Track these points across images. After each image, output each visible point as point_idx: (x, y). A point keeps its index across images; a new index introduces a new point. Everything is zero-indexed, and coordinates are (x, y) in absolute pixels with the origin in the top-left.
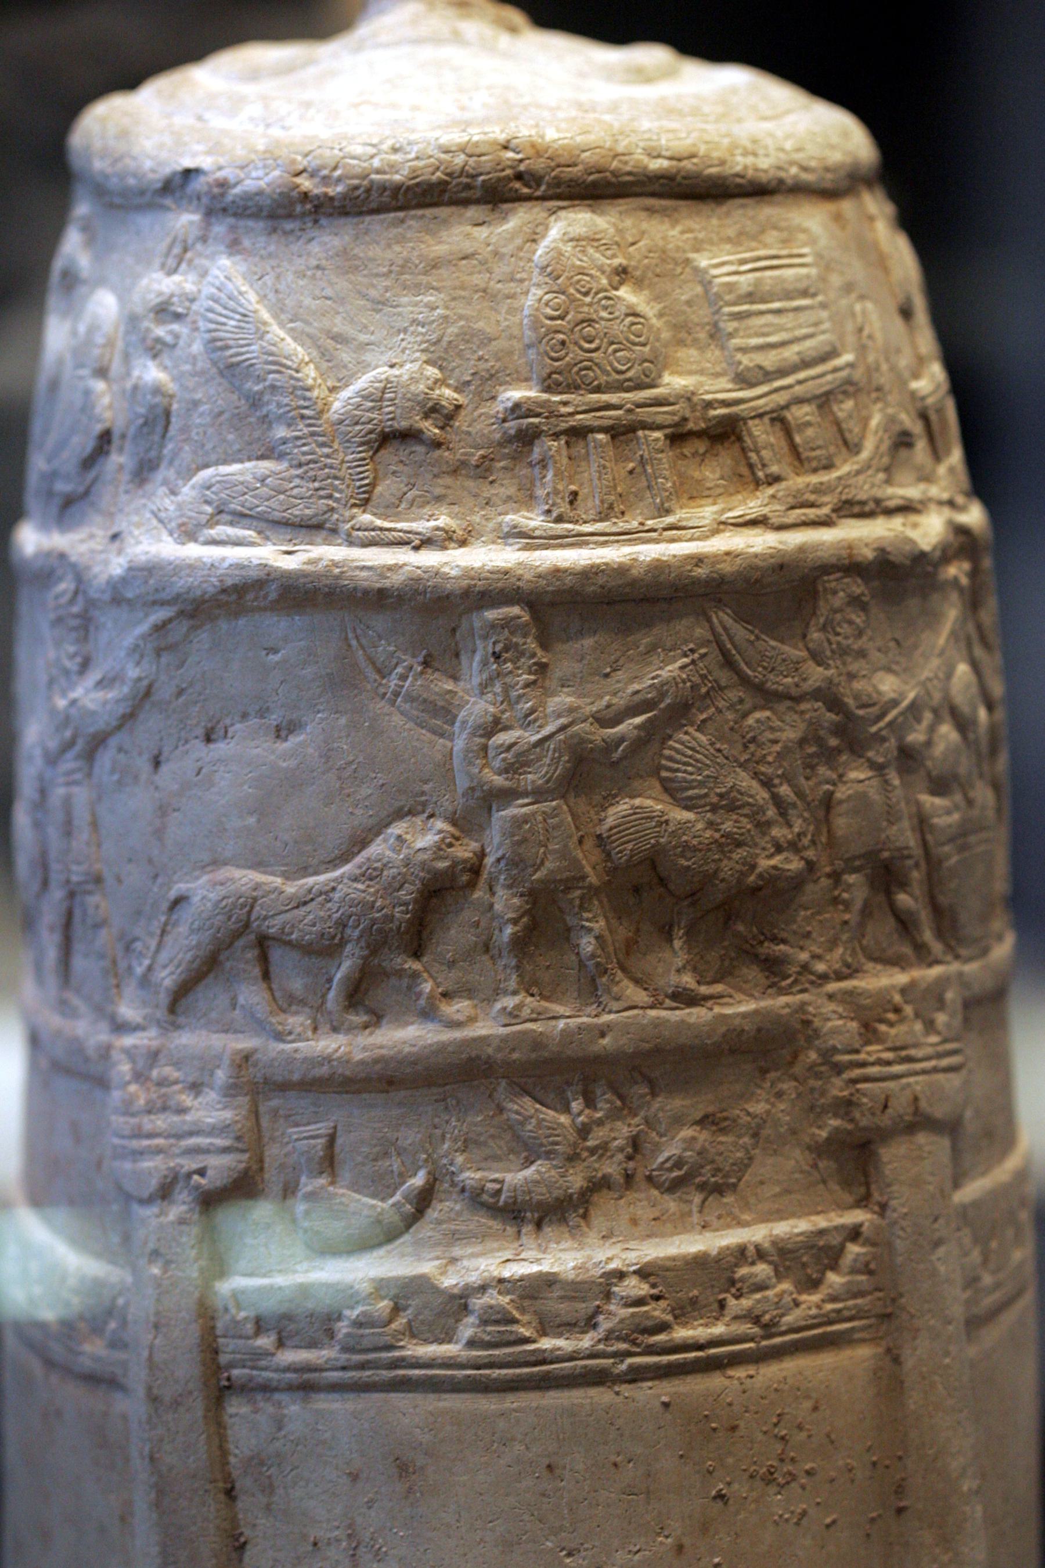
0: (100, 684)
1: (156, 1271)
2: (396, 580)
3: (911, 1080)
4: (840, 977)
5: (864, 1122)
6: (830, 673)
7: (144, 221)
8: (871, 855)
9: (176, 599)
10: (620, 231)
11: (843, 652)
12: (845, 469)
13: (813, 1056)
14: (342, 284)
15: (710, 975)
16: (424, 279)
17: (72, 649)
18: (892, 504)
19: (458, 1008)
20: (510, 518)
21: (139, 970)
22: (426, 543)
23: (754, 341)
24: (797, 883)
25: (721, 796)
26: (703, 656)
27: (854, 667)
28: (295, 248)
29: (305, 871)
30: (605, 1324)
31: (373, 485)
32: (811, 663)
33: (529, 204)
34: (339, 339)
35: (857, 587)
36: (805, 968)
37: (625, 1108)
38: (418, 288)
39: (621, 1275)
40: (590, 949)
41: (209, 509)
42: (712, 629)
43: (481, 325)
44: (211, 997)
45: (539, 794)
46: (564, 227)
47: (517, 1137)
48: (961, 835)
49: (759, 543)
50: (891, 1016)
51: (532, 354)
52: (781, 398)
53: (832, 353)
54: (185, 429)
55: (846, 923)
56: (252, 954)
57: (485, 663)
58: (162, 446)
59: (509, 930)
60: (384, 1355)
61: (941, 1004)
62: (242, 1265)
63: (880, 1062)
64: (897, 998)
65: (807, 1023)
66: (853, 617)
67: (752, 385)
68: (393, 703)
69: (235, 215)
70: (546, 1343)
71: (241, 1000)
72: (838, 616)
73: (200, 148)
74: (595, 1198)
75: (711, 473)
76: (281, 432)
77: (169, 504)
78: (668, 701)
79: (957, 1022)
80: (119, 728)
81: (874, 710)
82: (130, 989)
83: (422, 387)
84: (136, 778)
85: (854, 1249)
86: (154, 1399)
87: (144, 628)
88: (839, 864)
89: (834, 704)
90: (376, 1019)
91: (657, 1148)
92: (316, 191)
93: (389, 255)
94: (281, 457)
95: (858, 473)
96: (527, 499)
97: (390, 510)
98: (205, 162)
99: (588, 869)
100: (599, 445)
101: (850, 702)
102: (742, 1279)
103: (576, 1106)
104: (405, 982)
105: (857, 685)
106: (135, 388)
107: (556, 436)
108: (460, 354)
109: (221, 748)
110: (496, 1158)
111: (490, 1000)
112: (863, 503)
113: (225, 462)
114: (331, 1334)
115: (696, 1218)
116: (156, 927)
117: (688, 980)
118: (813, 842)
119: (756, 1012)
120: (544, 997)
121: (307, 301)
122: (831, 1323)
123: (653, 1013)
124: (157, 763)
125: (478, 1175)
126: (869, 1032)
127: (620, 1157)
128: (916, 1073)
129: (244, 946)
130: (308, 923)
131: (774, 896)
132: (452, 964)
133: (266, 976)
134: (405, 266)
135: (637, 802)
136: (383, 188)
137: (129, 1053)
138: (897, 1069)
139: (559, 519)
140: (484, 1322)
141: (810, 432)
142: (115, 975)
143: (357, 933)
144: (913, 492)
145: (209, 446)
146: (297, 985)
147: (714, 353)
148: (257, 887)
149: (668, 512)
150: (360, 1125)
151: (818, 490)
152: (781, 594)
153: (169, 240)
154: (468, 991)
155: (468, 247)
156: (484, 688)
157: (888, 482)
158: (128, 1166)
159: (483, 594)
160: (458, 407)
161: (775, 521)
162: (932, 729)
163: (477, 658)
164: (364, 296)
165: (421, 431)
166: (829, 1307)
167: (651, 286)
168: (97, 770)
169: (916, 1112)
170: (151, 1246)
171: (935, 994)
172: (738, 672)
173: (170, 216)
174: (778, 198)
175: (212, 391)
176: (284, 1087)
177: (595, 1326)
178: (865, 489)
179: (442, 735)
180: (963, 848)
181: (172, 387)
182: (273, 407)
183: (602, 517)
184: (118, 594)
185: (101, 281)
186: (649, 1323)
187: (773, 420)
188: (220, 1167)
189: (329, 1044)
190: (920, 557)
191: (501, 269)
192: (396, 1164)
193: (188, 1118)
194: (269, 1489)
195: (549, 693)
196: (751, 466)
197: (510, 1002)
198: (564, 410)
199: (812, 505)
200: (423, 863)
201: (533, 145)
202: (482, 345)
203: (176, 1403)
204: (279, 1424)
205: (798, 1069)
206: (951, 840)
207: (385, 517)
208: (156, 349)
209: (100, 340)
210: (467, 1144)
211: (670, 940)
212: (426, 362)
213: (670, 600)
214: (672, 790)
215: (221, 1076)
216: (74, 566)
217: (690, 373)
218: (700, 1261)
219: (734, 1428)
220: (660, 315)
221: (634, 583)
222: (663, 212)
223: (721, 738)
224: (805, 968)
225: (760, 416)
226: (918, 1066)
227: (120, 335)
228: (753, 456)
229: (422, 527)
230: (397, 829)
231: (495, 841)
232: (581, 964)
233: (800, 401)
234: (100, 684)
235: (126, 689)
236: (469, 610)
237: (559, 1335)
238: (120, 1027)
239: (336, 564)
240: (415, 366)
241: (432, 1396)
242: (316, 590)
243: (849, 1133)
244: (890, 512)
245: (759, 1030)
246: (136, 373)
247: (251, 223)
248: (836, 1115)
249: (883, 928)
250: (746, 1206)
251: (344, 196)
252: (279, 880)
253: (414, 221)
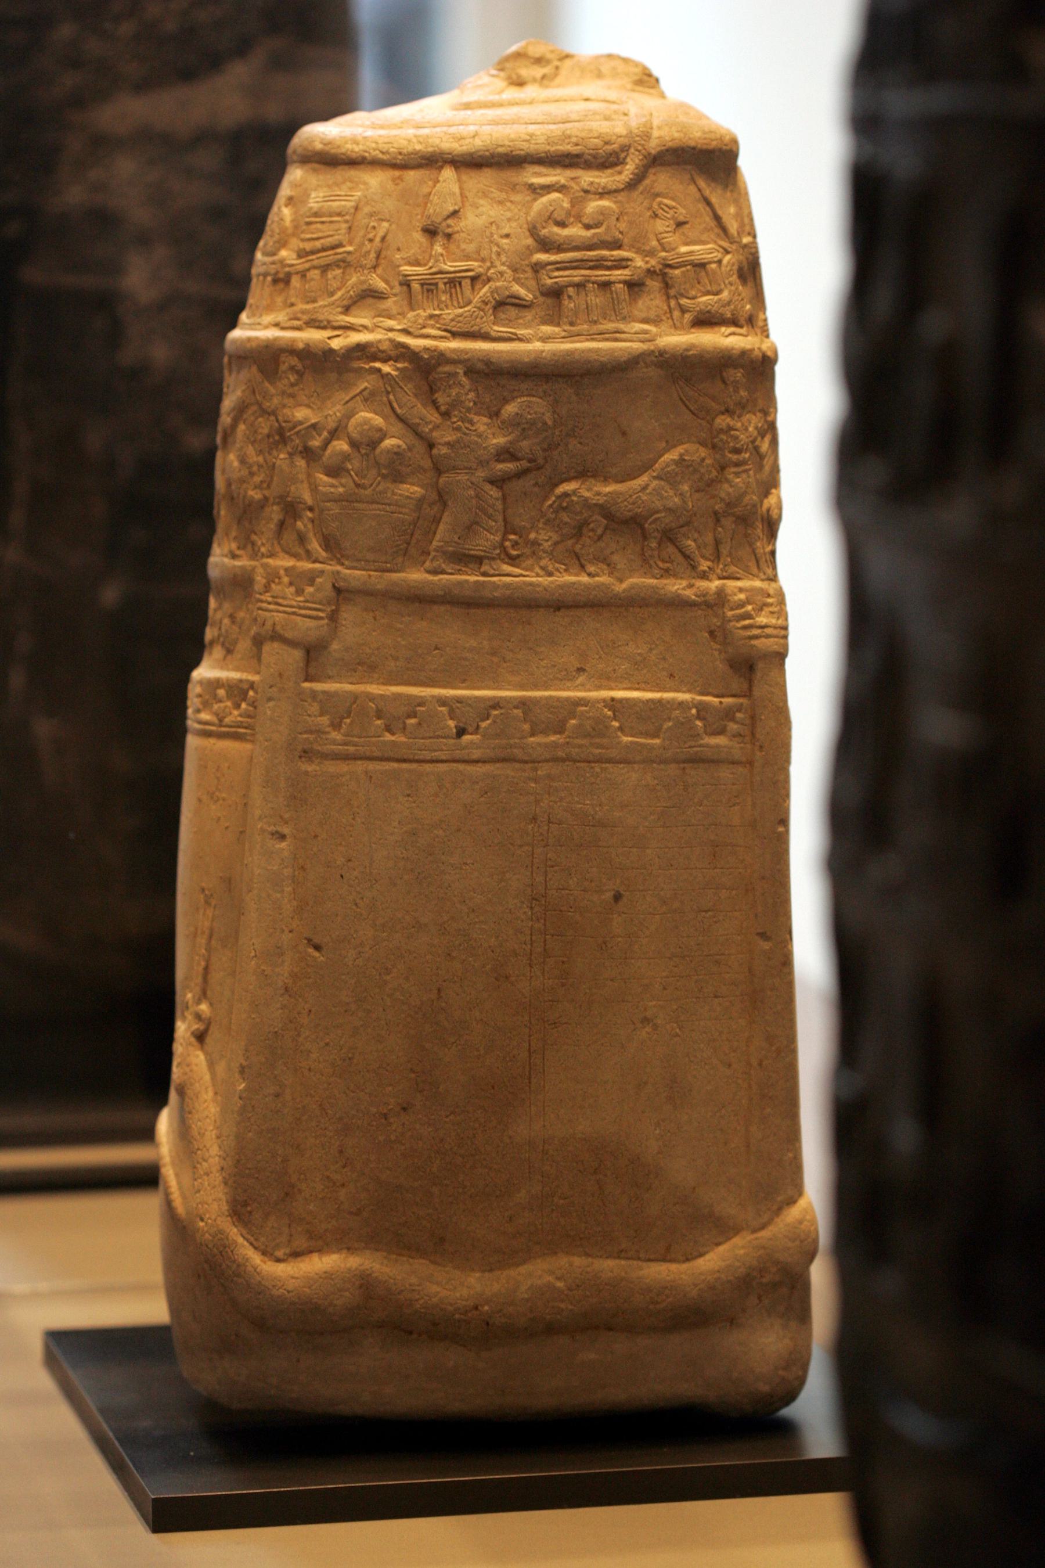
3: (275, 614)
18: (335, 324)
23: (309, 236)
27: (286, 401)
35: (294, 361)
50: (277, 580)
52: (307, 265)
53: (340, 245)
61: (311, 582)
64: (282, 572)
75: (279, 300)
81: (290, 425)
95: (325, 306)
112: (321, 321)
122: (239, 727)
128: (278, 611)
138: (272, 607)
141: (312, 283)
151: (303, 312)
162: (327, 443)
166: (239, 719)
169: (273, 630)
171: (311, 578)
174: (362, 166)
206: (335, 501)
225: (297, 273)
226: (281, 608)
233: (315, 267)
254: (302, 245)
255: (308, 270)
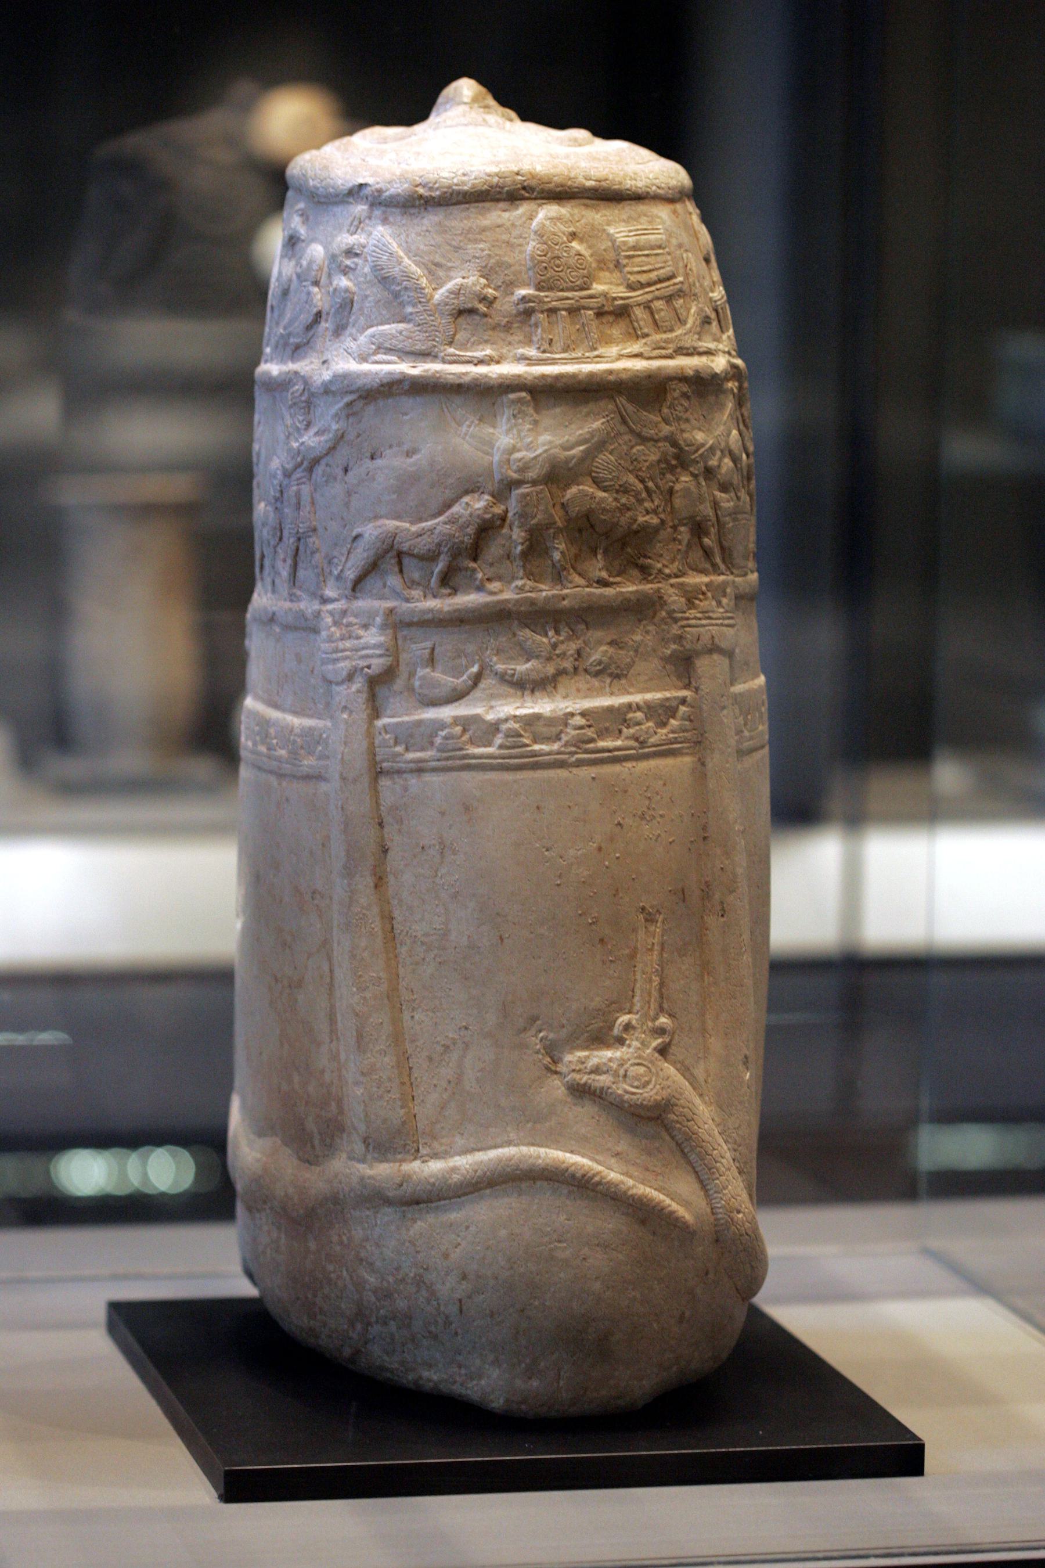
0: (317, 434)
1: (345, 716)
2: (467, 379)
4: (677, 576)
5: (688, 647)
6: (673, 429)
7: (338, 210)
8: (692, 518)
9: (357, 390)
10: (572, 215)
11: (679, 419)
12: (679, 332)
13: (664, 614)
14: (439, 239)
15: (615, 573)
16: (478, 237)
17: (301, 418)
18: (701, 350)
19: (495, 586)
20: (521, 351)
21: (336, 573)
22: (481, 362)
23: (636, 269)
24: (656, 530)
25: (620, 486)
26: (612, 419)
27: (683, 426)
28: (415, 221)
29: (421, 520)
30: (565, 738)
31: (454, 335)
32: (663, 424)
33: (528, 202)
34: (437, 265)
35: (685, 388)
36: (660, 571)
37: (574, 635)
38: (476, 241)
39: (572, 715)
40: (558, 558)
41: (374, 347)
42: (617, 406)
43: (506, 259)
44: (373, 583)
45: (534, 483)
46: (546, 213)
47: (523, 649)
48: (735, 513)
49: (639, 365)
50: (701, 597)
51: (531, 273)
52: (649, 297)
54: (361, 309)
55: (679, 550)
56: (393, 561)
57: (509, 420)
58: (349, 317)
59: (519, 548)
60: (458, 753)
62: (388, 712)
63: (695, 618)
64: (704, 588)
65: (661, 598)
66: (683, 402)
67: (634, 290)
68: (464, 439)
69: (386, 206)
70: (537, 747)
71: (389, 583)
72: (676, 402)
73: (365, 174)
74: (559, 679)
75: (616, 332)
76: (409, 309)
77: (353, 345)
78: (596, 439)
79: (732, 603)
80: (326, 454)
81: (694, 448)
82: (331, 582)
83: (478, 288)
84: (335, 479)
85: (683, 709)
86: (344, 779)
87: (341, 404)
88: (676, 522)
89: (674, 444)
90: (455, 591)
91: (589, 655)
92: (426, 194)
93: (462, 225)
94: (409, 321)
95: (685, 334)
96: (529, 342)
97: (463, 346)
98: (370, 180)
99: (557, 519)
100: (562, 316)
101: (681, 442)
102: (630, 719)
103: (551, 633)
104: (469, 573)
105: (686, 435)
106: (335, 290)
107: (542, 312)
108: (496, 273)
109: (379, 462)
110: (512, 658)
111: (510, 582)
112: (688, 349)
113: (382, 324)
114: (432, 744)
115: (607, 690)
116: (345, 551)
117: (604, 574)
118: (664, 511)
119: (637, 591)
120: (536, 581)
121: (422, 247)
122: (672, 743)
123: (588, 590)
124: (346, 470)
125: (504, 667)
126: (690, 603)
127: (571, 659)
129: (391, 557)
130: (423, 545)
131: (644, 536)
132: (492, 565)
133: (401, 571)
134: (470, 230)
135: (581, 487)
136: (459, 193)
137: (331, 613)
138: (704, 622)
139: (544, 352)
140: (507, 736)
141: (662, 314)
142: (322, 577)
143: (446, 549)
144: (712, 345)
145: (373, 317)
146: (416, 576)
147: (617, 275)
148: (397, 528)
149: (595, 349)
150: (446, 642)
152: (648, 391)
153: (351, 219)
154: (500, 578)
155: (499, 221)
156: (508, 431)
157: (699, 339)
158: (330, 667)
159: (508, 386)
160: (495, 298)
161: (646, 355)
162: (720, 460)
163: (505, 417)
164: (450, 245)
165: (477, 309)
166: (671, 735)
167: (587, 242)
168: (314, 476)
169: (713, 643)
170: (343, 704)
172: (629, 427)
173: (351, 206)
175: (375, 290)
176: (410, 625)
177: (560, 739)
178: (689, 342)
179: (488, 454)
180: (735, 520)
181: (354, 289)
182: (406, 298)
183: (564, 351)
184: (327, 390)
185: (314, 240)
186: (586, 738)
187: (645, 307)
188: (378, 664)
189: (432, 603)
190: (715, 376)
191: (516, 232)
192: (464, 661)
193: (362, 641)
194: (400, 821)
195: (539, 434)
196: (634, 329)
197: (520, 583)
198: (546, 300)
199: (664, 348)
200: (479, 516)
201: (531, 173)
202: (507, 268)
203: (355, 781)
204: (406, 789)
205: (656, 620)
206: (730, 515)
207: (460, 350)
208: (345, 271)
209: (315, 267)
210: (498, 652)
211: (596, 555)
212: (481, 276)
213: (596, 391)
214: (597, 482)
215: (378, 620)
216: (303, 377)
217: (606, 283)
218: (610, 709)
219: (626, 792)
220: (592, 256)
221: (580, 382)
222: (593, 207)
223: (621, 458)
224: (660, 571)
225: (639, 305)
226: (714, 622)
227: (326, 263)
228: (636, 324)
229: (479, 354)
230: (466, 499)
231: (513, 505)
232: (554, 565)
234: (317, 434)
235: (331, 435)
236: (501, 394)
237: (542, 743)
238: (325, 601)
239: (437, 372)
240: (475, 278)
241: (481, 773)
242: (428, 384)
243: (681, 652)
244: (700, 354)
245: (638, 600)
246: (335, 283)
247: (394, 210)
248: (675, 643)
249: (696, 555)
250: (632, 685)
251: (440, 197)
252: (407, 525)
253: (473, 208)
254: (632, 278)
255: (651, 301)
